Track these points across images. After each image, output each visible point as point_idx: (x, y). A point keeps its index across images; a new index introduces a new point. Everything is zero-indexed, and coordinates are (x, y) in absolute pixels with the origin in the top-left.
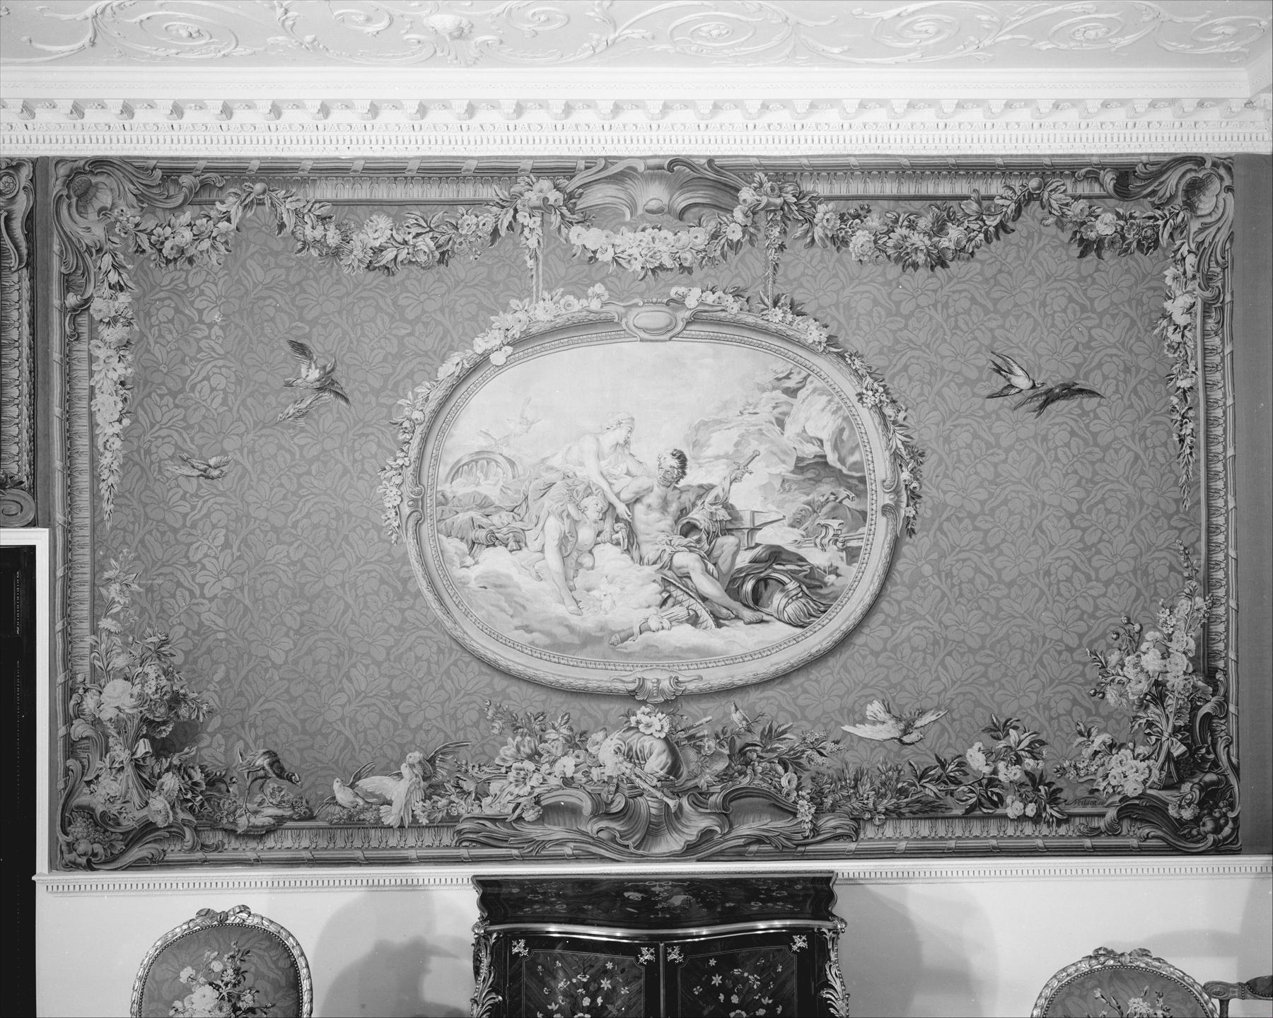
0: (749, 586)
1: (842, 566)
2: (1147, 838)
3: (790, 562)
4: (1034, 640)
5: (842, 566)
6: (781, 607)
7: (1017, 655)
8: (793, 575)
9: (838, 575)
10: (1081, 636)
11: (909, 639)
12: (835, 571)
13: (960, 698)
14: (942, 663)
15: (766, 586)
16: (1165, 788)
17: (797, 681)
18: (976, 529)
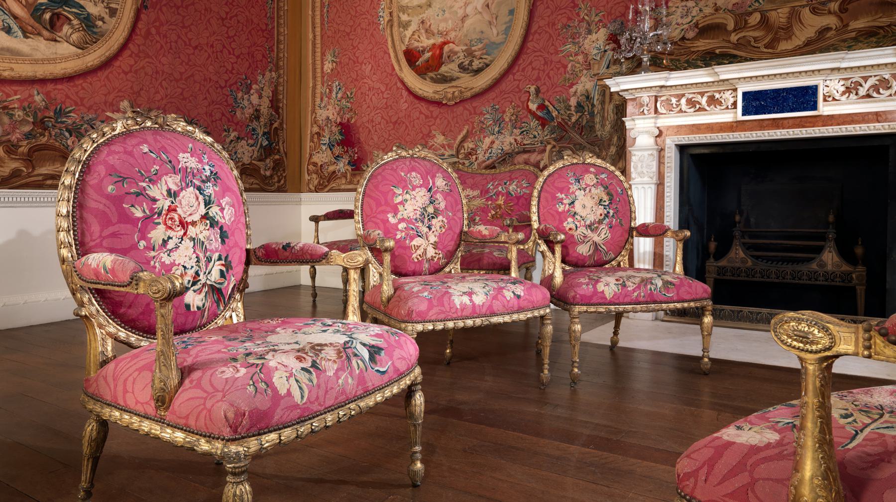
0: (47, 16)
1: (107, 17)
2: (252, 184)
3: (75, 7)
4: (205, 80)
5: (107, 17)
6: (69, 34)
7: (198, 86)
8: (77, 16)
9: (104, 22)
10: (226, 81)
11: (143, 68)
12: (102, 19)
13: (169, 105)
14: (161, 84)
15: (58, 18)
16: (260, 160)
17: (79, 82)
18: (179, 14)
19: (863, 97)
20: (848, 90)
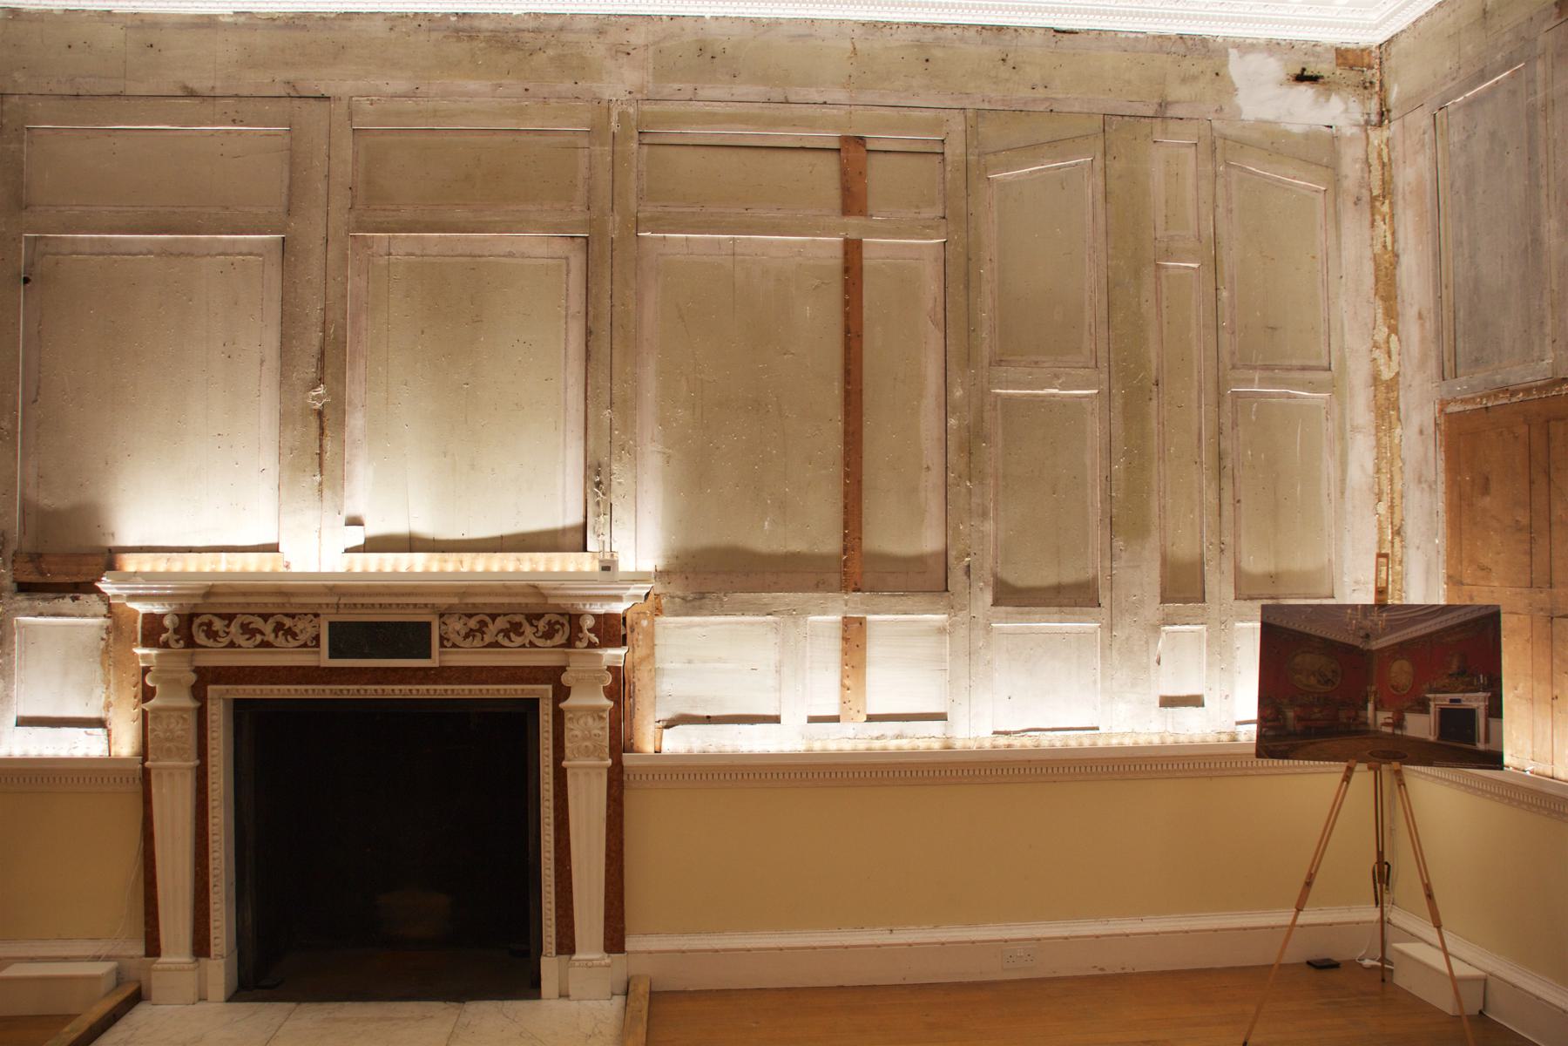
19: (490, 645)
20: (470, 634)
